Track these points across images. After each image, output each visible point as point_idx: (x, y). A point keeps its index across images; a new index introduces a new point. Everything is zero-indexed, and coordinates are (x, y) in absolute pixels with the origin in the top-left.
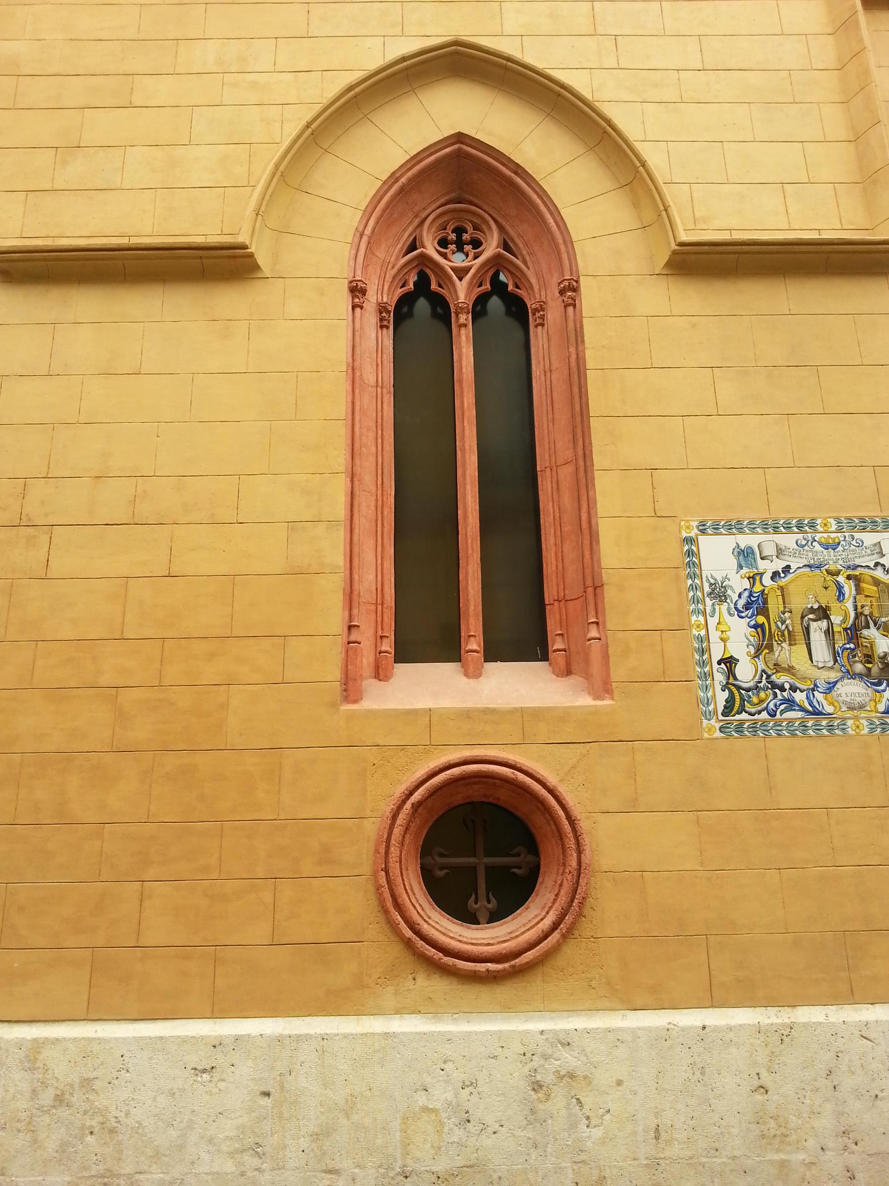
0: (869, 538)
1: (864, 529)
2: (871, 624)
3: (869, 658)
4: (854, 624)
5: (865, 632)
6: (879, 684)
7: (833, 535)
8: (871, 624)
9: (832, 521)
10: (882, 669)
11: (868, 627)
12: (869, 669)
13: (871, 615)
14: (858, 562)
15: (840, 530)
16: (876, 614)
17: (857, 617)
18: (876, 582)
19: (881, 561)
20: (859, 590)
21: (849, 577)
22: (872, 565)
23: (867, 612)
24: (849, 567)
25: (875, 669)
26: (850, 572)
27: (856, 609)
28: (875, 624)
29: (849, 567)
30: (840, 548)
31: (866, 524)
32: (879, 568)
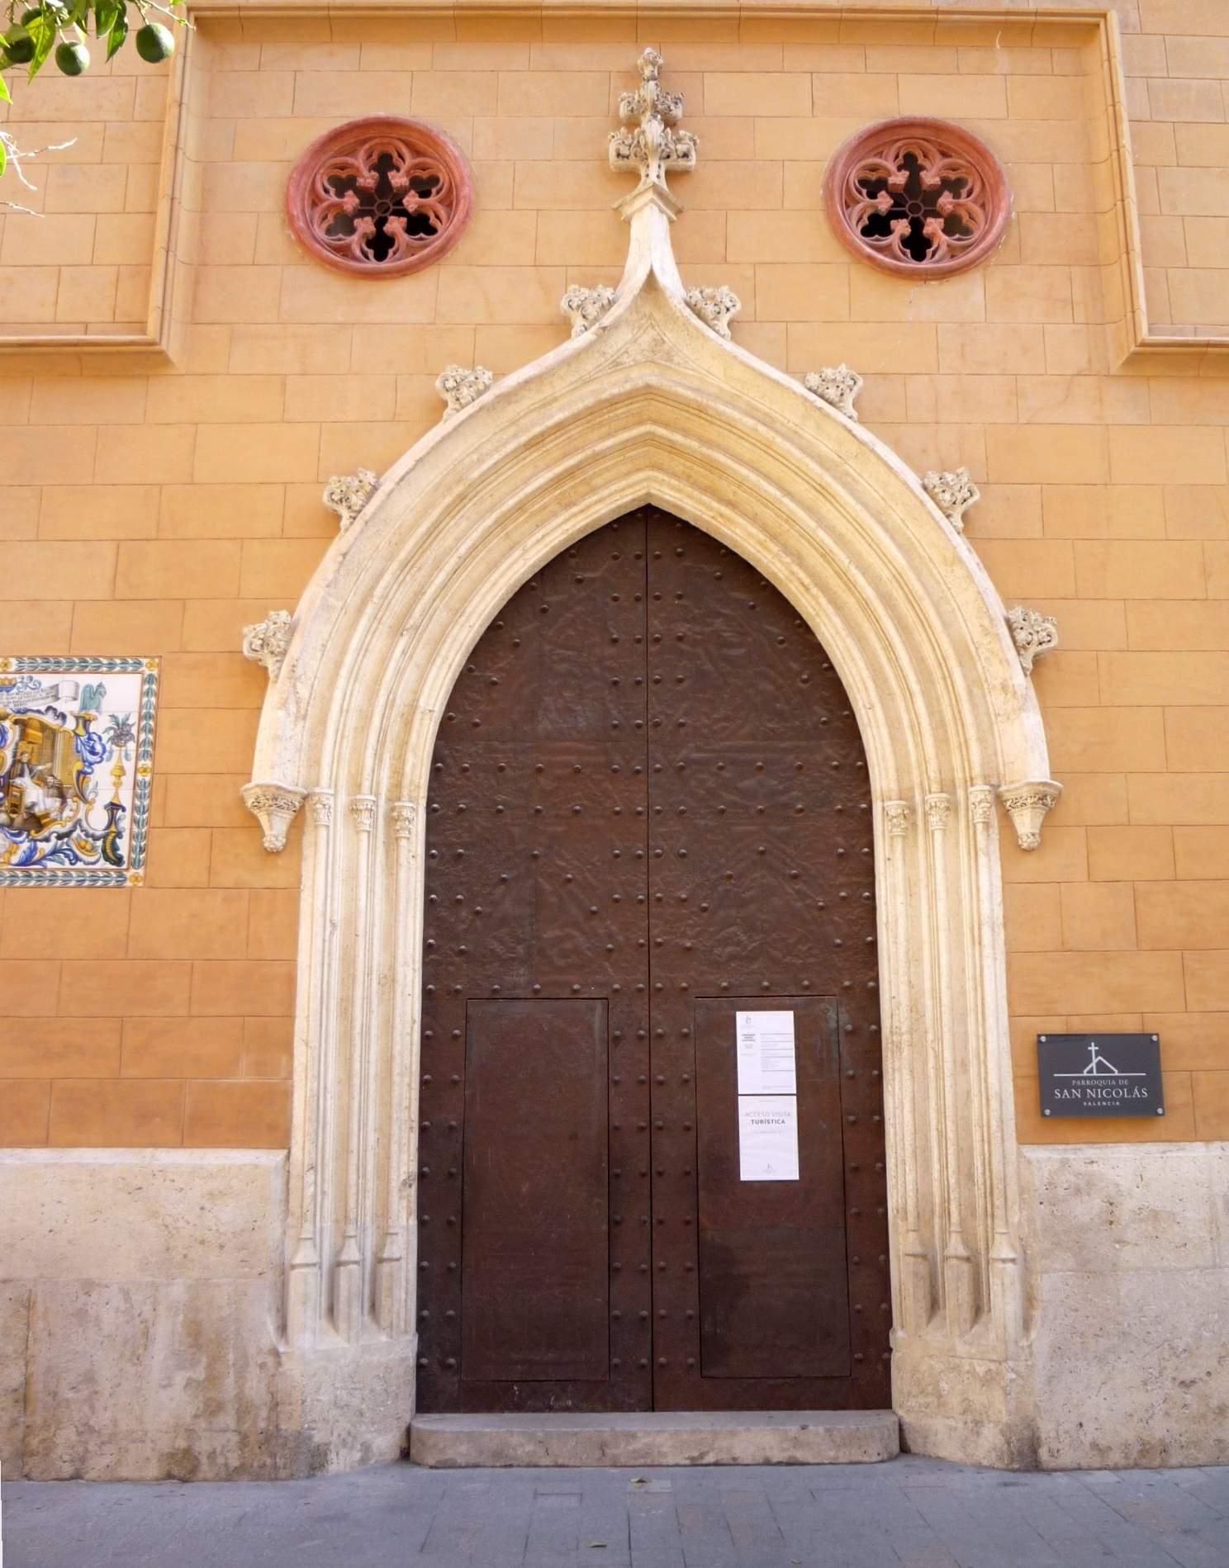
0: (47, 680)
1: (45, 671)
2: (27, 771)
3: (15, 808)
4: (9, 773)
5: (18, 781)
6: (18, 835)
7: (10, 676)
8: (27, 771)
9: (13, 661)
10: (25, 820)
11: (21, 775)
12: (12, 820)
13: (29, 763)
14: (30, 706)
15: (18, 672)
16: (34, 762)
17: (13, 765)
18: (44, 727)
19: (54, 705)
20: (23, 735)
21: (16, 722)
22: (43, 709)
23: (25, 759)
24: (19, 712)
25: (19, 819)
26: (19, 716)
27: (15, 756)
28: (31, 771)
29: (19, 712)
30: (15, 691)
31: (51, 664)
32: (51, 713)
